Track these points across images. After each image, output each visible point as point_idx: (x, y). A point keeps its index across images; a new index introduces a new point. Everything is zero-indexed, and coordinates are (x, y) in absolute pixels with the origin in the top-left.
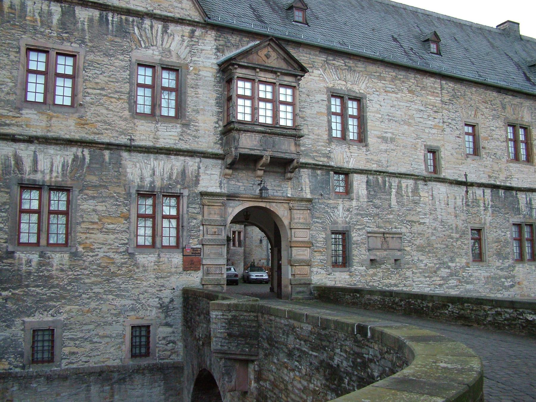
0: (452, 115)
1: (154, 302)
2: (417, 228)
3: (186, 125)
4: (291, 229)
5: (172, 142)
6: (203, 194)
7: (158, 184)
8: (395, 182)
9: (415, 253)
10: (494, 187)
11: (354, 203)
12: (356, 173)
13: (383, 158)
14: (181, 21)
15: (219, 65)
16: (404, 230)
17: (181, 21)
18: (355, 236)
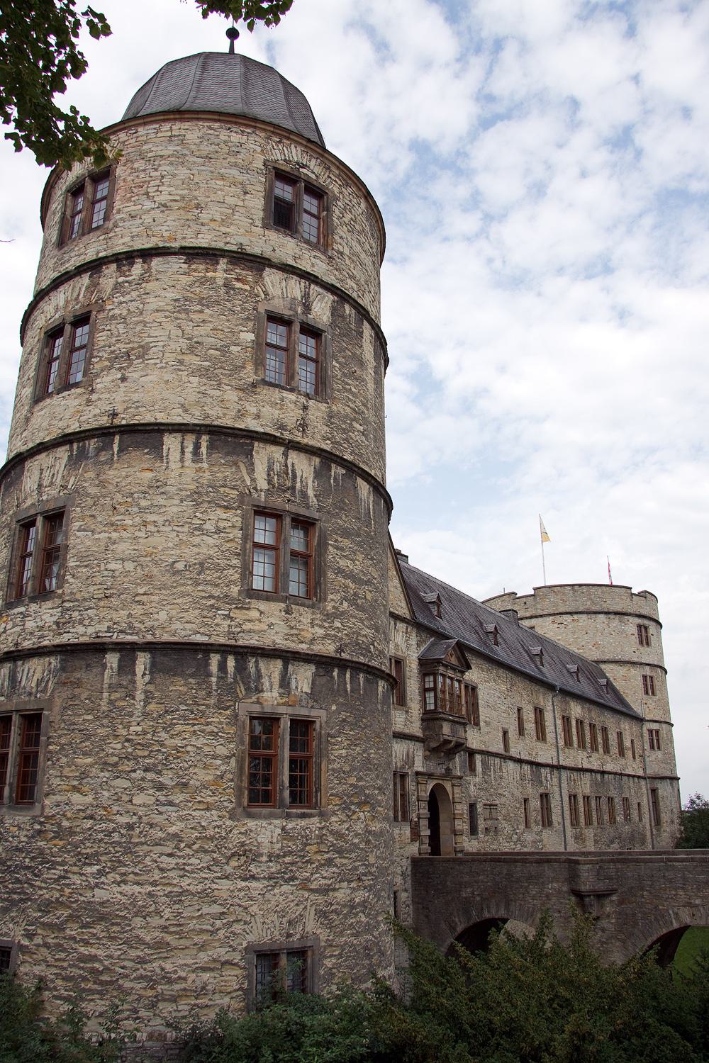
0: (513, 701)
1: (399, 870)
2: (503, 800)
3: (407, 712)
4: (453, 803)
5: (402, 727)
6: (417, 773)
7: (399, 765)
8: (492, 759)
9: (503, 822)
10: (531, 763)
11: (477, 779)
12: (479, 753)
13: (486, 738)
14: (403, 620)
15: (419, 659)
16: (497, 802)
17: (403, 620)
18: (480, 808)
